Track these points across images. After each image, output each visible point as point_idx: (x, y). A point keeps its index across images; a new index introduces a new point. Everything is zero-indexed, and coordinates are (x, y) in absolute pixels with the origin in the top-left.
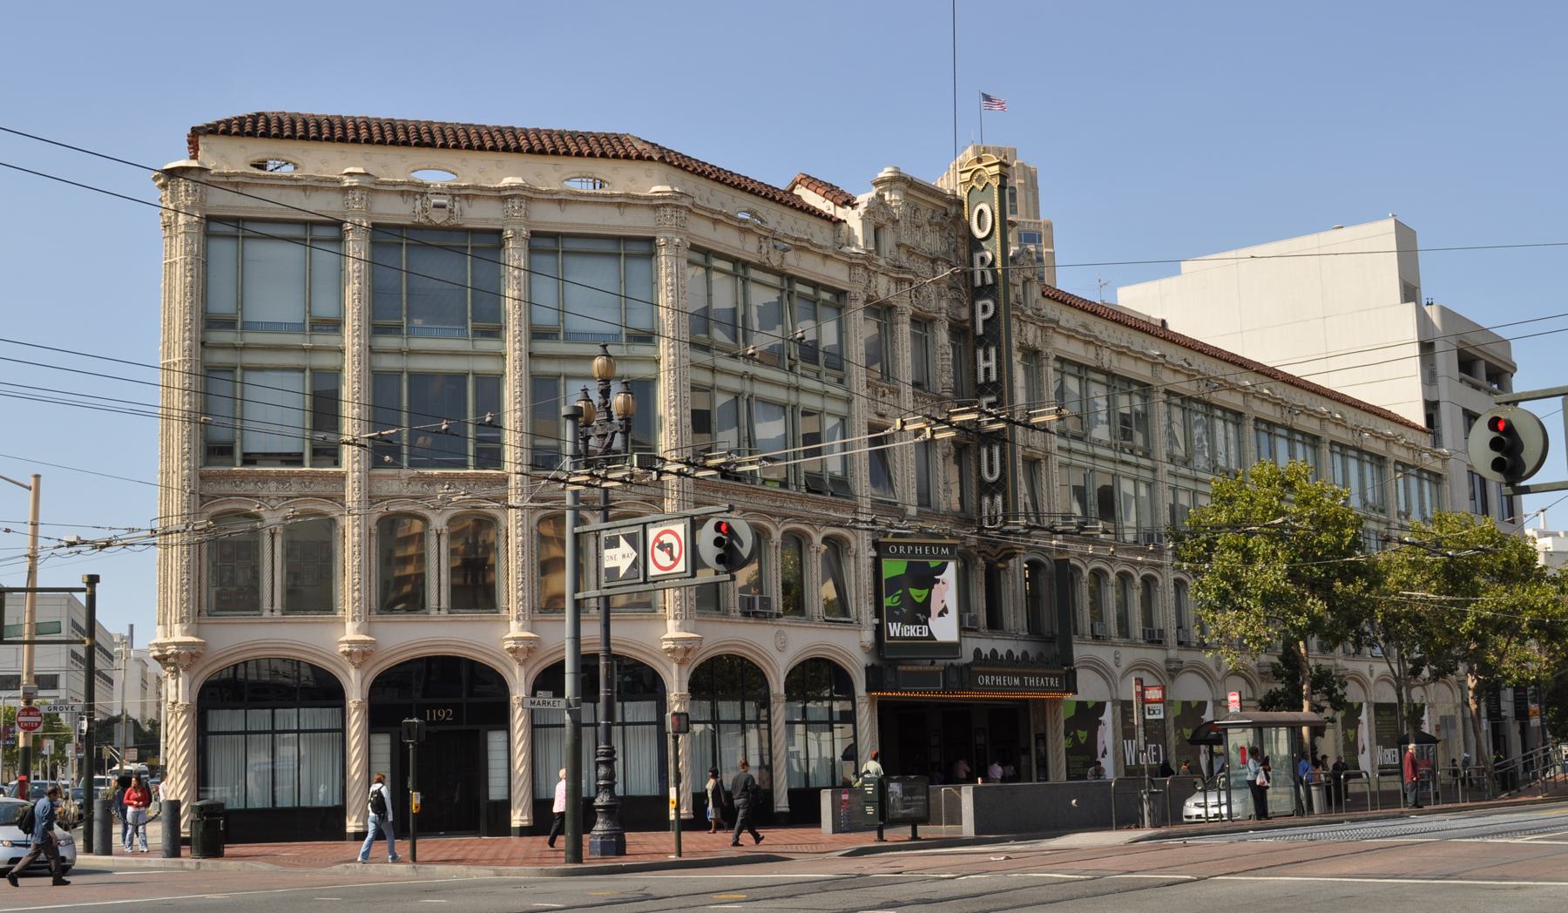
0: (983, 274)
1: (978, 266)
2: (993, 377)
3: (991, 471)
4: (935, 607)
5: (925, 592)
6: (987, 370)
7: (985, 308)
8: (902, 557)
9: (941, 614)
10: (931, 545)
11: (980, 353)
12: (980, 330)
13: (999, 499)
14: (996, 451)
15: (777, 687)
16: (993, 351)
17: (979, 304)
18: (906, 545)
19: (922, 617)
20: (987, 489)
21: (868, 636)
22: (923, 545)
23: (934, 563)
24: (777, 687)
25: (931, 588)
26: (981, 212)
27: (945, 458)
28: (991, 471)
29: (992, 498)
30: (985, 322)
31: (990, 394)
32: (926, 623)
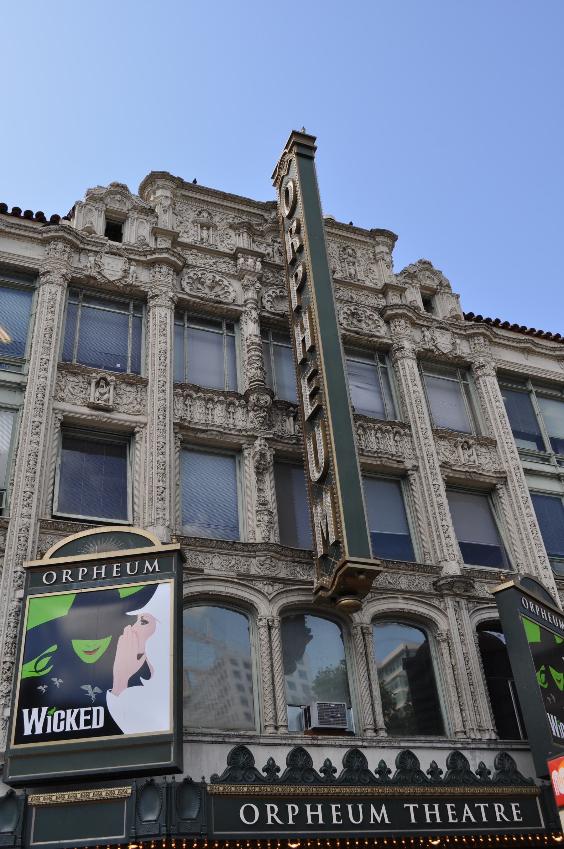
4: (123, 667)
5: (104, 644)
6: (304, 341)
8: (67, 586)
9: (134, 681)
19: (91, 691)
23: (127, 590)
25: (117, 634)
27: (260, 471)
32: (101, 701)
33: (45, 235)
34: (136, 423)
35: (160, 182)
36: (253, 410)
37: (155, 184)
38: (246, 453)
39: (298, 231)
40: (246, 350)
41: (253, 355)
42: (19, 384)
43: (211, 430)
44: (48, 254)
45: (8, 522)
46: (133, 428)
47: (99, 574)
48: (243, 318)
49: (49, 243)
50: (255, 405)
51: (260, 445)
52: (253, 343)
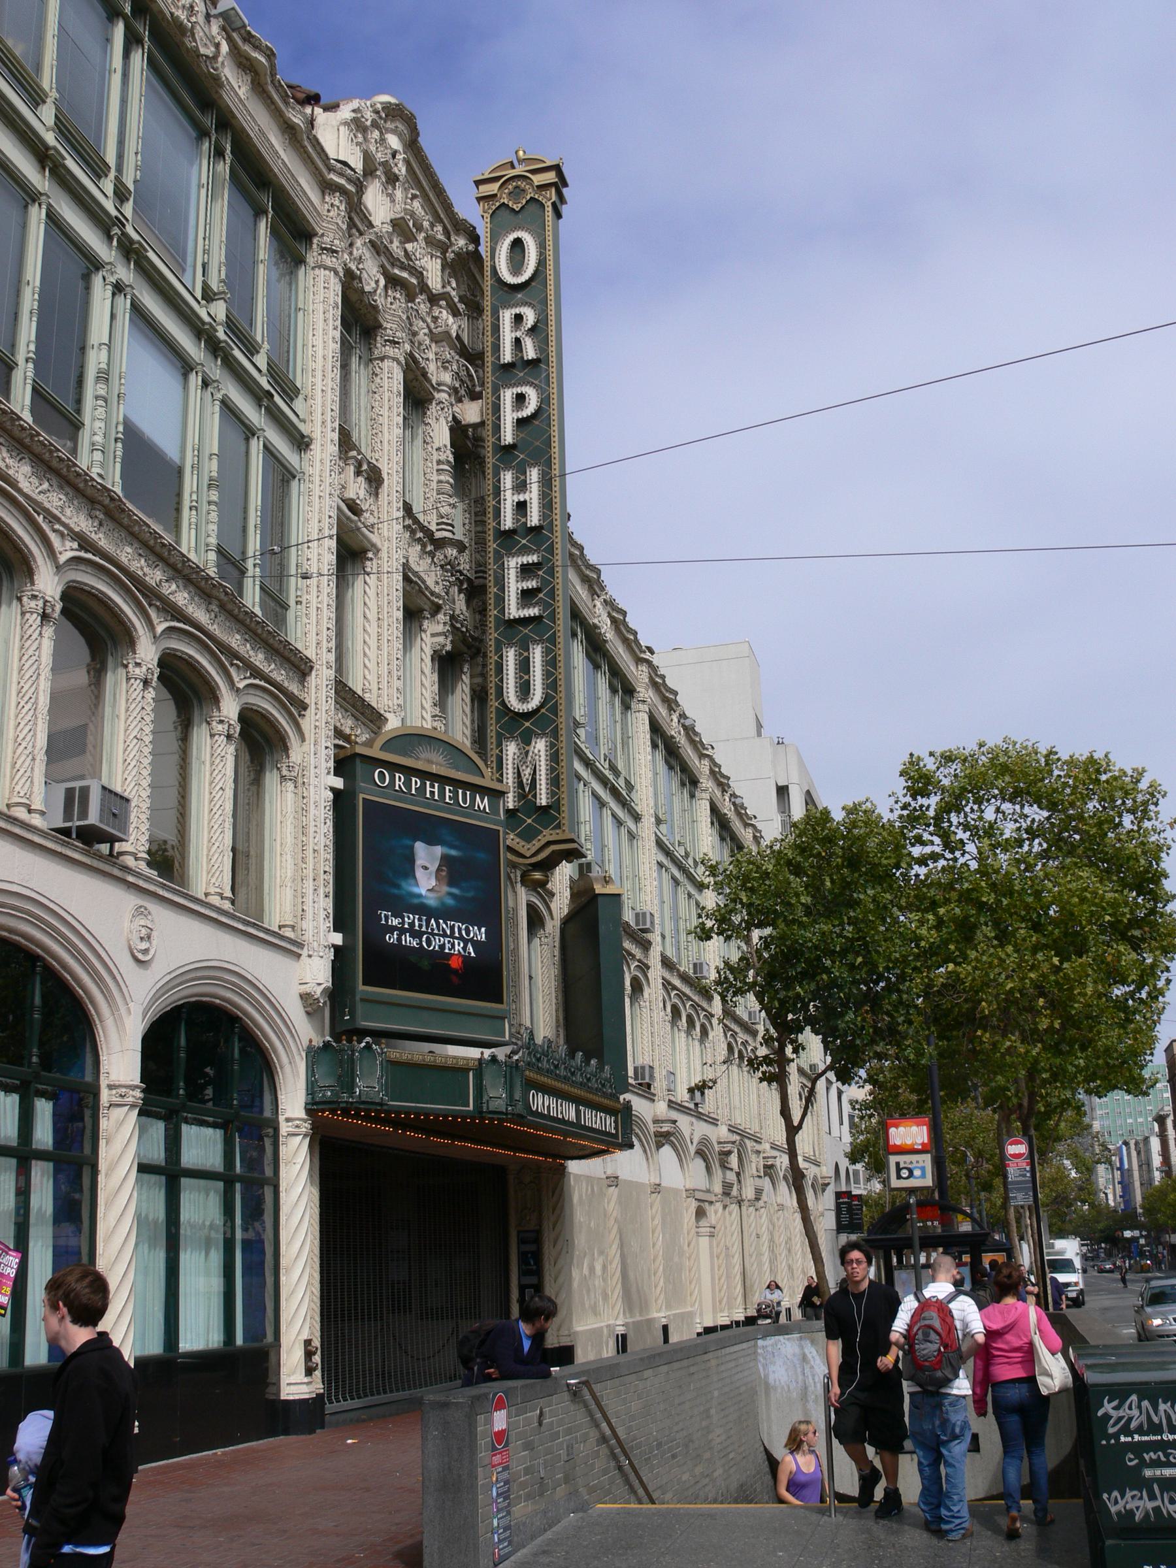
0: (518, 342)
1: (508, 335)
2: (534, 518)
3: (524, 690)
6: (521, 507)
7: (520, 399)
10: (456, 783)
11: (507, 479)
12: (508, 437)
13: (540, 746)
14: (537, 655)
15: (120, 1062)
16: (534, 474)
17: (508, 396)
18: (409, 771)
20: (520, 725)
21: (317, 972)
22: (443, 780)
24: (120, 1062)
26: (518, 244)
28: (524, 690)
29: (526, 740)
30: (520, 423)
31: (525, 550)
33: (333, 177)
34: (374, 545)
35: (401, 127)
36: (442, 566)
37: (392, 121)
38: (426, 623)
39: (533, 330)
40: (436, 467)
41: (448, 482)
42: (303, 436)
43: (416, 583)
44: (329, 211)
45: (312, 668)
46: (365, 551)
47: (432, 793)
48: (433, 409)
49: (334, 191)
50: (449, 563)
51: (445, 623)
52: (448, 462)
